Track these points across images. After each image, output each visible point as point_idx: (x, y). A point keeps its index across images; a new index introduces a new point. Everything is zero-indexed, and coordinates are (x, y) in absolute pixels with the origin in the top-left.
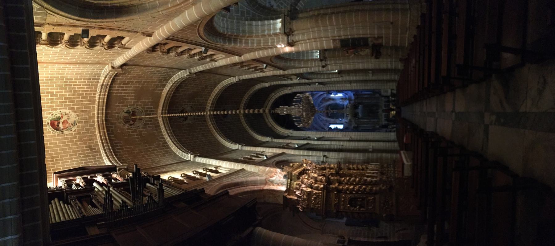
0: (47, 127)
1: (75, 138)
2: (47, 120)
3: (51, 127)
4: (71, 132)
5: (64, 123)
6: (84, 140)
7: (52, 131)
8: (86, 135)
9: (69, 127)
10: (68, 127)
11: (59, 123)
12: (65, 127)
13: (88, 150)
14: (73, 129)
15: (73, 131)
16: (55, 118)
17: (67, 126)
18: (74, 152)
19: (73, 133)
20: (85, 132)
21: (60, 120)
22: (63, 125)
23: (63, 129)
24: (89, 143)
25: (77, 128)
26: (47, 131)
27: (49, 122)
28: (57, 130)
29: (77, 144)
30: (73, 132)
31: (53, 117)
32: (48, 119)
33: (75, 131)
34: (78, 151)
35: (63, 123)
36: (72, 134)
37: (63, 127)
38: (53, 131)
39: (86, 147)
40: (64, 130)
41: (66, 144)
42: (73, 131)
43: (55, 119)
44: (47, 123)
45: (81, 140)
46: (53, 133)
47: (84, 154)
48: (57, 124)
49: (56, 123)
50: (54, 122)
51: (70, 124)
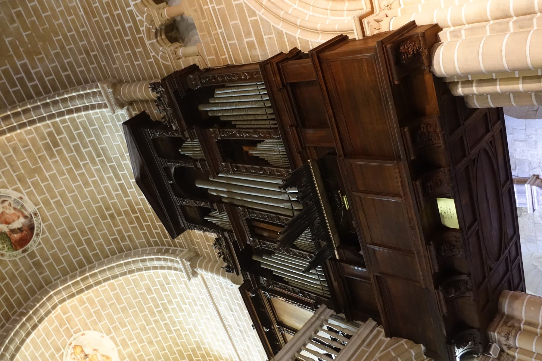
0: (34, 249)
1: (35, 184)
2: (19, 257)
3: (31, 242)
4: (26, 198)
5: (8, 221)
6: (35, 162)
7: (41, 237)
8: (18, 163)
9: (13, 205)
10: (15, 209)
11: (13, 231)
12: (19, 214)
13: (60, 152)
14: (15, 195)
15: (20, 195)
16: (5, 245)
17: (13, 211)
18: (75, 180)
19: (24, 192)
20: (12, 166)
21: (5, 233)
22: (14, 221)
23: (26, 217)
24: (38, 151)
25: (7, 188)
26: (43, 245)
27: (21, 250)
28: (31, 228)
29: (53, 177)
30: (22, 193)
31: (6, 249)
32: (16, 257)
33: (17, 190)
34: (70, 171)
35: (8, 223)
36: (30, 194)
37: (19, 217)
38: (38, 234)
39: (52, 156)
40: (26, 213)
41: (59, 198)
42: (20, 195)
43: (8, 243)
44: (25, 254)
45: (38, 170)
46: (44, 233)
47: (73, 159)
48: (16, 233)
49: (16, 236)
50: (16, 241)
51: (3, 208)
